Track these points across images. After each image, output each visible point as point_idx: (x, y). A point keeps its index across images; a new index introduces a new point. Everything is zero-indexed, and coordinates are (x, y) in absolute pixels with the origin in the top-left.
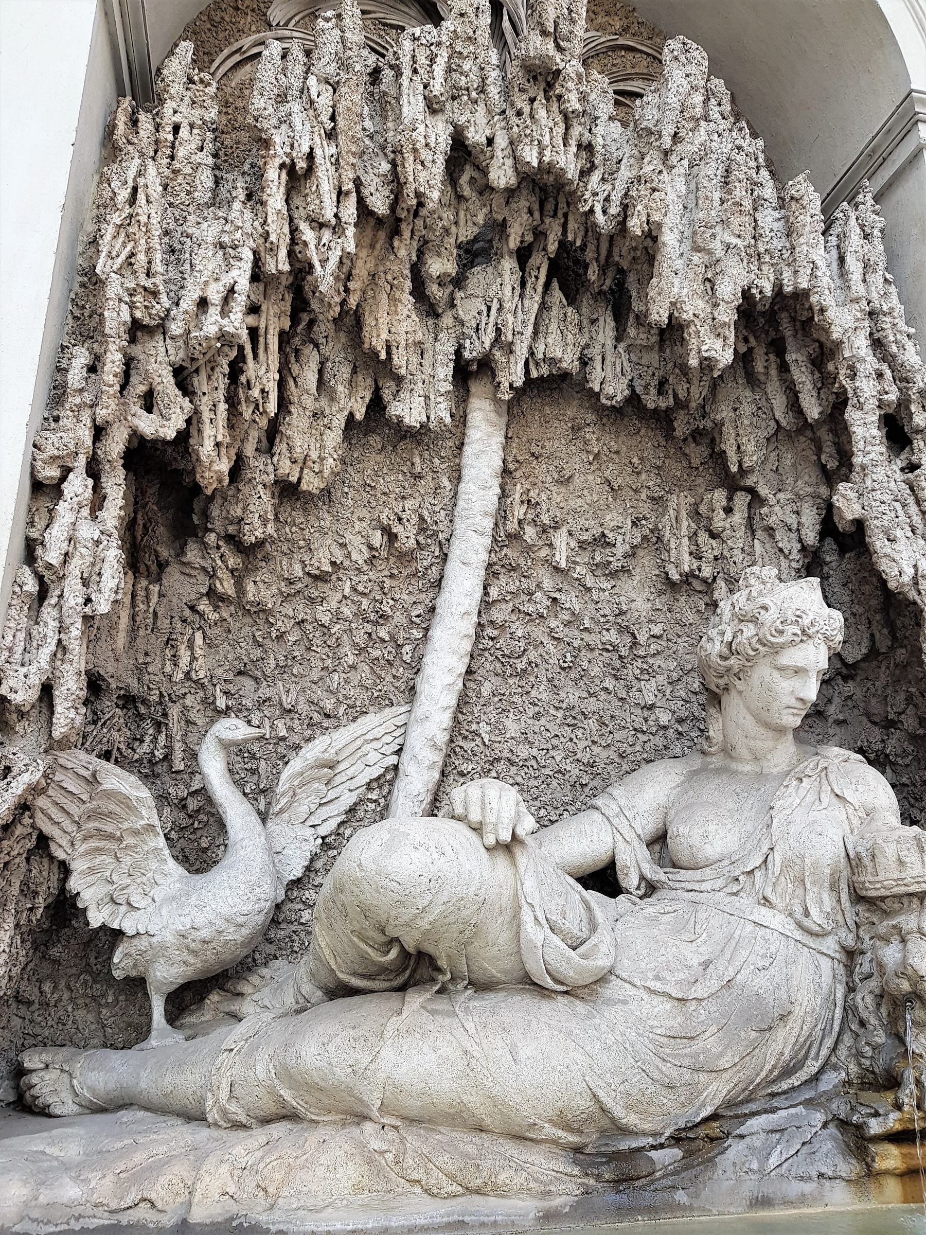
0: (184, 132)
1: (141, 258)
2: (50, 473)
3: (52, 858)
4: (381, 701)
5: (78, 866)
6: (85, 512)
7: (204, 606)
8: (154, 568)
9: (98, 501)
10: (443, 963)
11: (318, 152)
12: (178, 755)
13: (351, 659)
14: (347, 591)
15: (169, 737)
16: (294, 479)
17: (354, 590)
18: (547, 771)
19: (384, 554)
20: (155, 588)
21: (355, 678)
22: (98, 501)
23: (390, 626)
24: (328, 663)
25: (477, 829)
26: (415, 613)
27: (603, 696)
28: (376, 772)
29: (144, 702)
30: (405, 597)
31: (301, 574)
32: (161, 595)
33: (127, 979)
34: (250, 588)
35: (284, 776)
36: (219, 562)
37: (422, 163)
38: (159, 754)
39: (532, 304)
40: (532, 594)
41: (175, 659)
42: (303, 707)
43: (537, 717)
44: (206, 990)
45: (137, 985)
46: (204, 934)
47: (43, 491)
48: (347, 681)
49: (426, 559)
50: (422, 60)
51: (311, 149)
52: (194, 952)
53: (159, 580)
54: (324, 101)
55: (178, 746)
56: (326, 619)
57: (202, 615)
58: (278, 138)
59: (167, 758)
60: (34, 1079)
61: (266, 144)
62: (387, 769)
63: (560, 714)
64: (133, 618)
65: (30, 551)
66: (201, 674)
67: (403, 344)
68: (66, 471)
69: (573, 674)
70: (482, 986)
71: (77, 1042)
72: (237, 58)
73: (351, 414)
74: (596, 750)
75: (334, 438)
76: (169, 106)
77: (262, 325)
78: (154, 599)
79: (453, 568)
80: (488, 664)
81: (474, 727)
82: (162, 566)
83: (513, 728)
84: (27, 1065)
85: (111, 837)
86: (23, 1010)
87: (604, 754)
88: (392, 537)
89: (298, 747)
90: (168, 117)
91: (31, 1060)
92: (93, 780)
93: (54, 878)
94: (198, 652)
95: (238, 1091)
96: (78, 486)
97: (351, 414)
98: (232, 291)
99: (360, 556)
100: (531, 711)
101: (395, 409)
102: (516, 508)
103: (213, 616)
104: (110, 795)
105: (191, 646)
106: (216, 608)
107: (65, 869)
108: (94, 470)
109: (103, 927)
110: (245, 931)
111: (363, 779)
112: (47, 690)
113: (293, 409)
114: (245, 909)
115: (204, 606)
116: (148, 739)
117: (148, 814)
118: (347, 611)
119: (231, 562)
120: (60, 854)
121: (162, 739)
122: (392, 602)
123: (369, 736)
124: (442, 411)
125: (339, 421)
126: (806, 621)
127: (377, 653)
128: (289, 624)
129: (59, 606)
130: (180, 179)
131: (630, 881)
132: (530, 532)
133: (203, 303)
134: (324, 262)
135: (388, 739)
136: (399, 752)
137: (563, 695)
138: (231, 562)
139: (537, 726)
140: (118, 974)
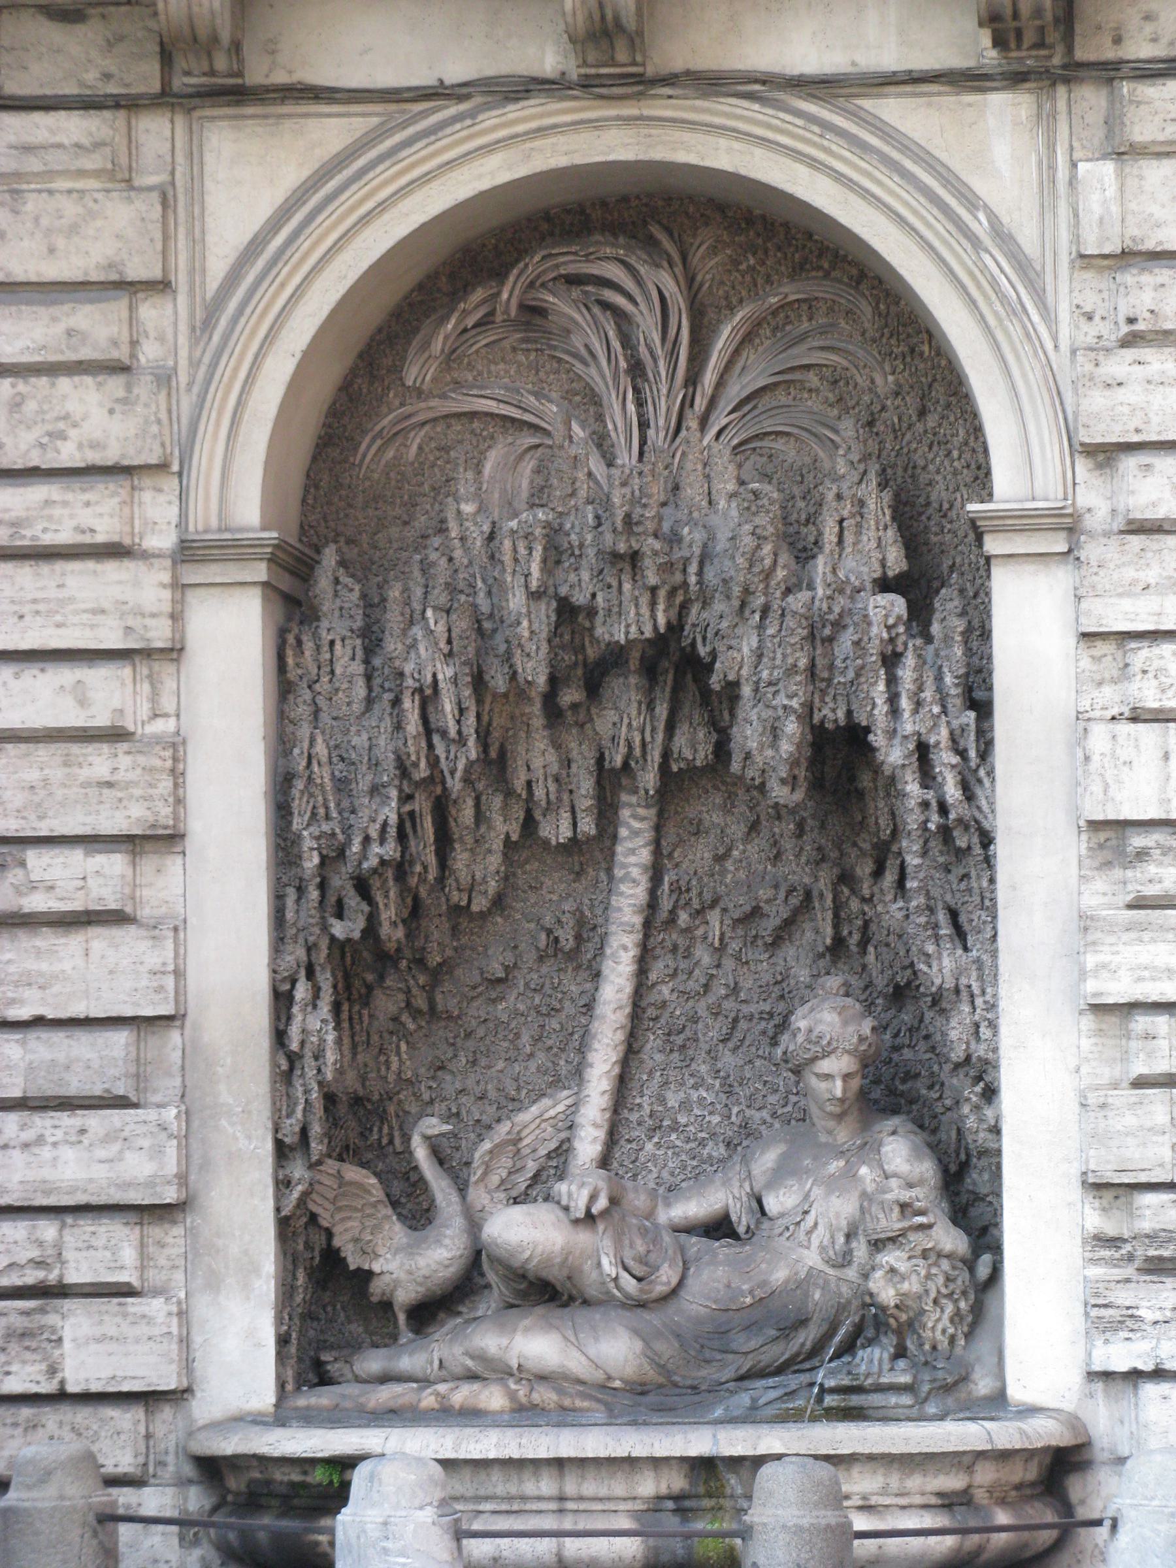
0: (338, 646)
1: (322, 811)
2: (286, 987)
3: (320, 1227)
4: (557, 1083)
5: (336, 1230)
6: (309, 1009)
7: (405, 1018)
8: (363, 991)
9: (316, 995)
10: (559, 1288)
11: (440, 677)
12: (397, 1141)
13: (528, 1049)
14: (522, 989)
15: (391, 1128)
16: (464, 903)
17: (527, 985)
18: (703, 1135)
19: (550, 951)
20: (365, 1012)
21: (533, 1065)
22: (316, 995)
23: (563, 1015)
24: (512, 1054)
25: (566, 1209)
26: (582, 1003)
27: (758, 1063)
28: (553, 1145)
29: (369, 1100)
30: (573, 988)
31: (478, 979)
32: (371, 1016)
33: (380, 1302)
34: (439, 998)
35: (477, 1155)
36: (412, 982)
37: (528, 655)
38: (385, 1141)
39: (662, 711)
40: (691, 973)
41: (388, 1064)
42: (492, 1094)
43: (695, 1087)
44: (430, 1311)
45: (387, 1306)
46: (425, 1272)
47: (282, 1000)
48: (526, 1068)
49: (589, 950)
50: (522, 551)
51: (434, 675)
52: (421, 1284)
53: (366, 1004)
54: (441, 629)
55: (396, 1133)
56: (505, 1018)
57: (404, 1025)
58: (409, 668)
59: (391, 1142)
60: (329, 1367)
61: (401, 674)
62: (562, 1142)
63: (717, 1083)
64: (353, 1036)
65: (280, 1036)
66: (409, 1074)
67: (542, 778)
68: (294, 982)
69: (731, 1045)
70: (586, 1302)
71: (354, 1347)
72: (379, 442)
73: (508, 836)
74: (748, 1113)
75: (495, 861)
76: (325, 624)
77: (417, 809)
78: (366, 1019)
79: (608, 967)
80: (652, 1043)
81: (638, 1101)
82: (370, 988)
83: (673, 1100)
84: (323, 1358)
85: (356, 1210)
86: (315, 1324)
87: (757, 1115)
88: (557, 940)
89: (489, 1127)
90: (326, 637)
91: (326, 1357)
92: (339, 1175)
93: (323, 1238)
94: (405, 1056)
95: (445, 1364)
96: (302, 991)
97: (508, 836)
98: (385, 825)
99: (530, 957)
100: (692, 1081)
101: (545, 830)
102: (665, 897)
103: (411, 1026)
104: (351, 1183)
105: (398, 1054)
106: (414, 1019)
107: (329, 1234)
108: (310, 974)
109: (359, 1269)
110: (452, 1269)
111: (543, 1152)
112: (304, 1132)
113: (457, 846)
114: (449, 1255)
115: (405, 1018)
116: (376, 1129)
117: (378, 1193)
118: (521, 1007)
119: (421, 982)
120: (325, 1224)
121: (386, 1130)
122: (560, 996)
123: (546, 1116)
124: (587, 826)
125: (498, 845)
126: (824, 1042)
127: (550, 1043)
128: (474, 1023)
129: (302, 1076)
130: (340, 694)
131: (741, 1230)
132: (683, 917)
133: (367, 840)
134: (452, 773)
135: (562, 1116)
136: (570, 1127)
137: (719, 1065)
138: (421, 982)
139: (695, 1096)
140: (375, 1299)
